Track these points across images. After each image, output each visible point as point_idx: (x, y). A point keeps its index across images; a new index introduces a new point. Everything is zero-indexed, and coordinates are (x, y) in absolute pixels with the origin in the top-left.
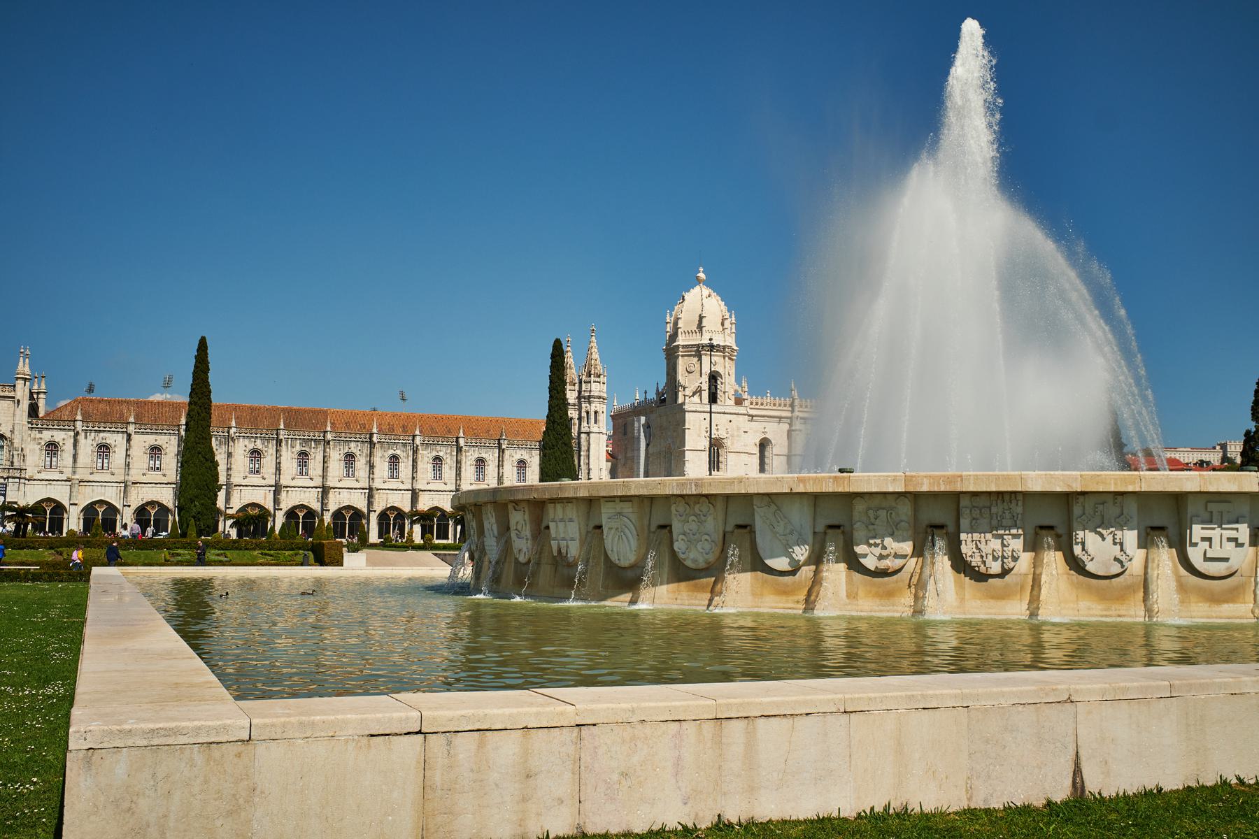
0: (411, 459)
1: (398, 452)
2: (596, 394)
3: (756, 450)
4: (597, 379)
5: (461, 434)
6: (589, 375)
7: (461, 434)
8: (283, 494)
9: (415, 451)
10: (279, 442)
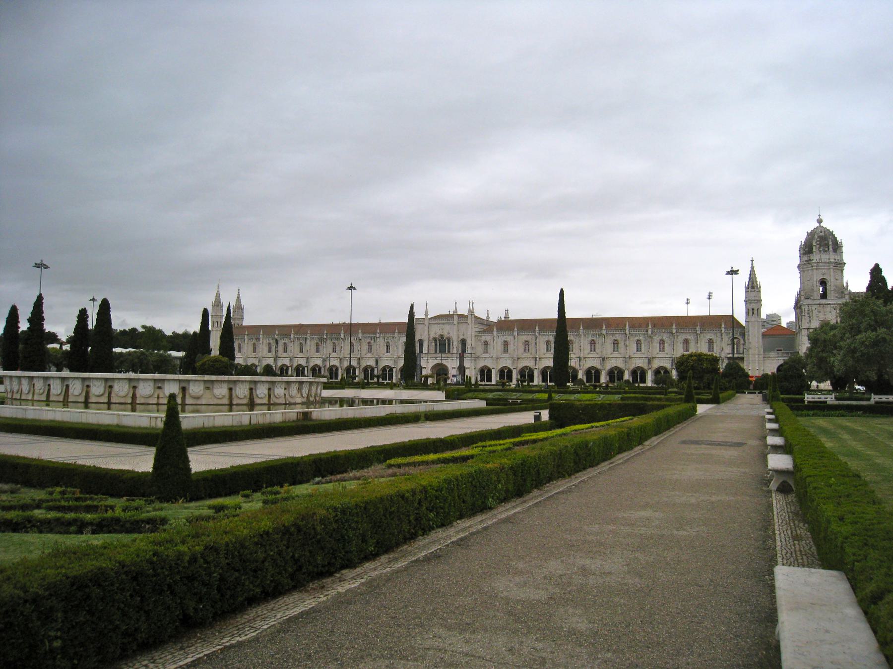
1: (641, 338)
4: (753, 290)
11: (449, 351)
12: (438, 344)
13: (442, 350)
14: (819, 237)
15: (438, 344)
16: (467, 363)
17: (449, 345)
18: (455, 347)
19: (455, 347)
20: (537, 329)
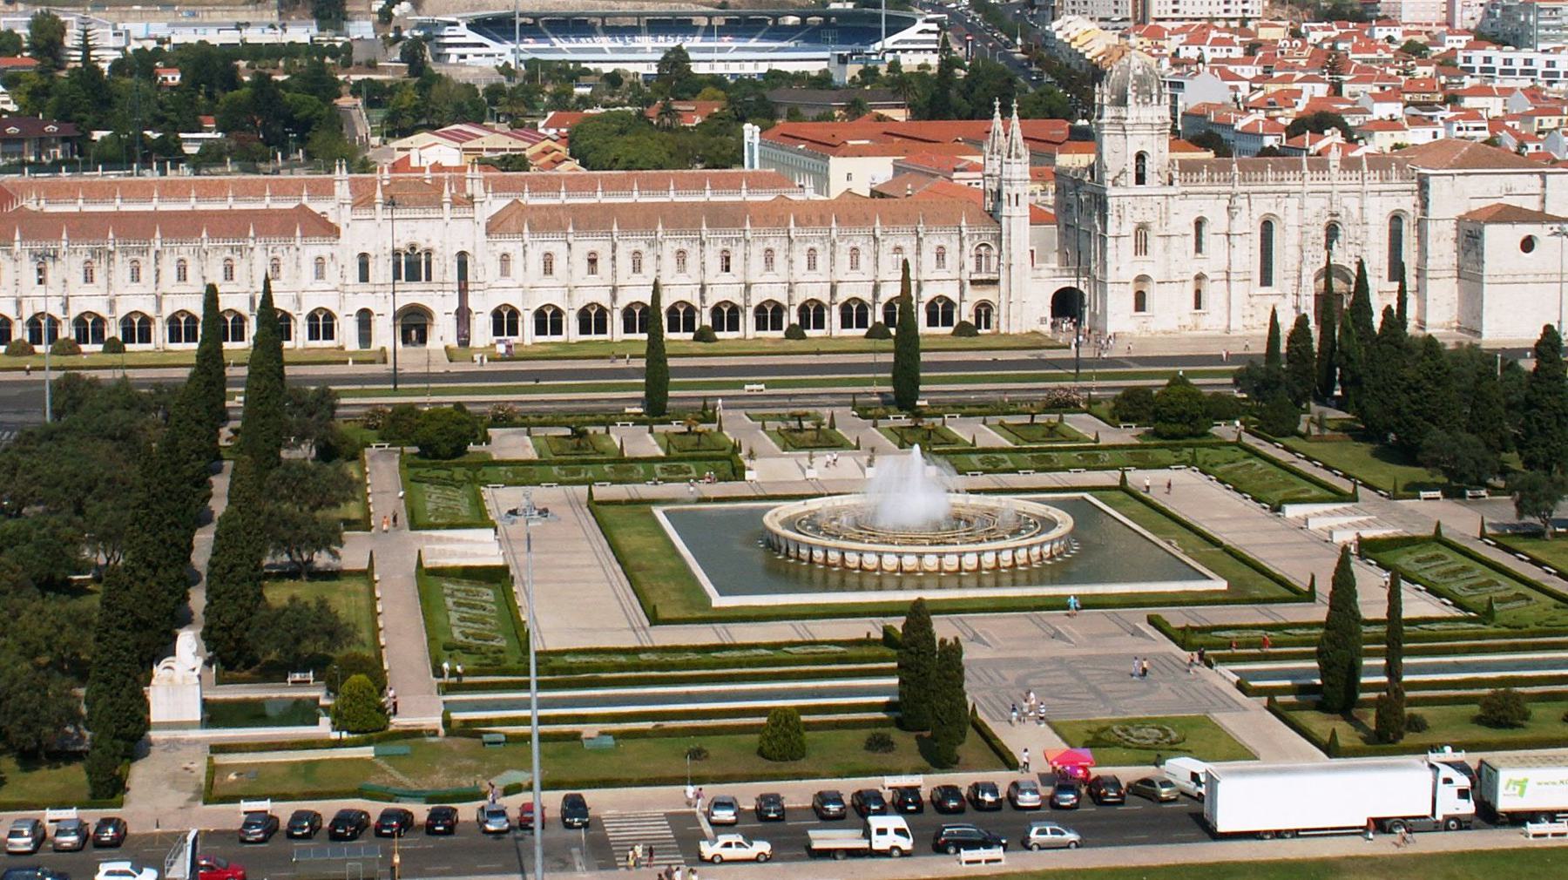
0: (828, 251)
1: (816, 245)
2: (1018, 177)
3: (1192, 231)
5: (878, 224)
6: (1009, 157)
7: (878, 224)
8: (708, 288)
9: (833, 244)
10: (702, 244)
11: (429, 278)
12: (403, 263)
13: (413, 276)
14: (1136, 77)
15: (403, 263)
16: (473, 302)
17: (429, 264)
18: (444, 268)
19: (444, 268)
20: (615, 229)
